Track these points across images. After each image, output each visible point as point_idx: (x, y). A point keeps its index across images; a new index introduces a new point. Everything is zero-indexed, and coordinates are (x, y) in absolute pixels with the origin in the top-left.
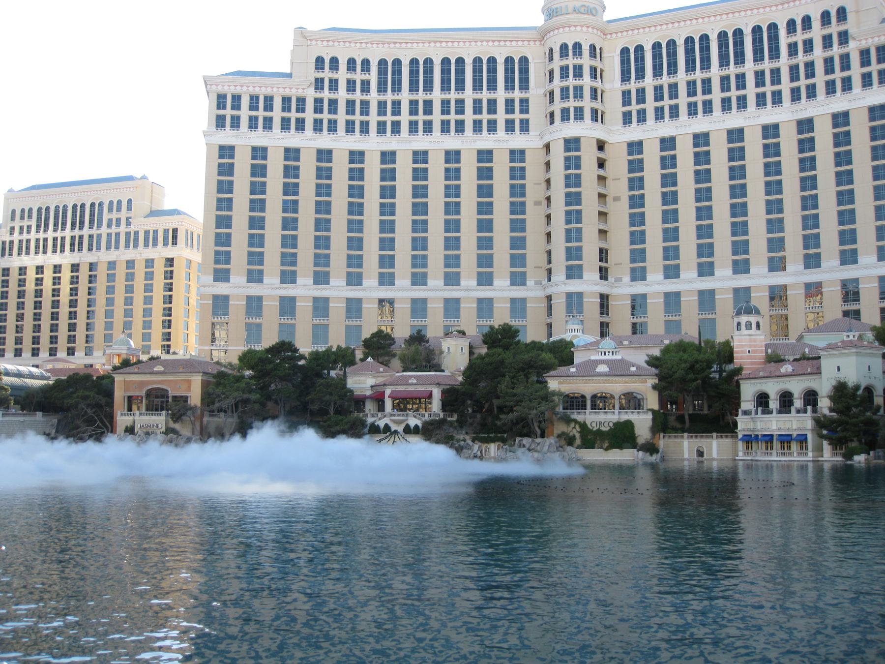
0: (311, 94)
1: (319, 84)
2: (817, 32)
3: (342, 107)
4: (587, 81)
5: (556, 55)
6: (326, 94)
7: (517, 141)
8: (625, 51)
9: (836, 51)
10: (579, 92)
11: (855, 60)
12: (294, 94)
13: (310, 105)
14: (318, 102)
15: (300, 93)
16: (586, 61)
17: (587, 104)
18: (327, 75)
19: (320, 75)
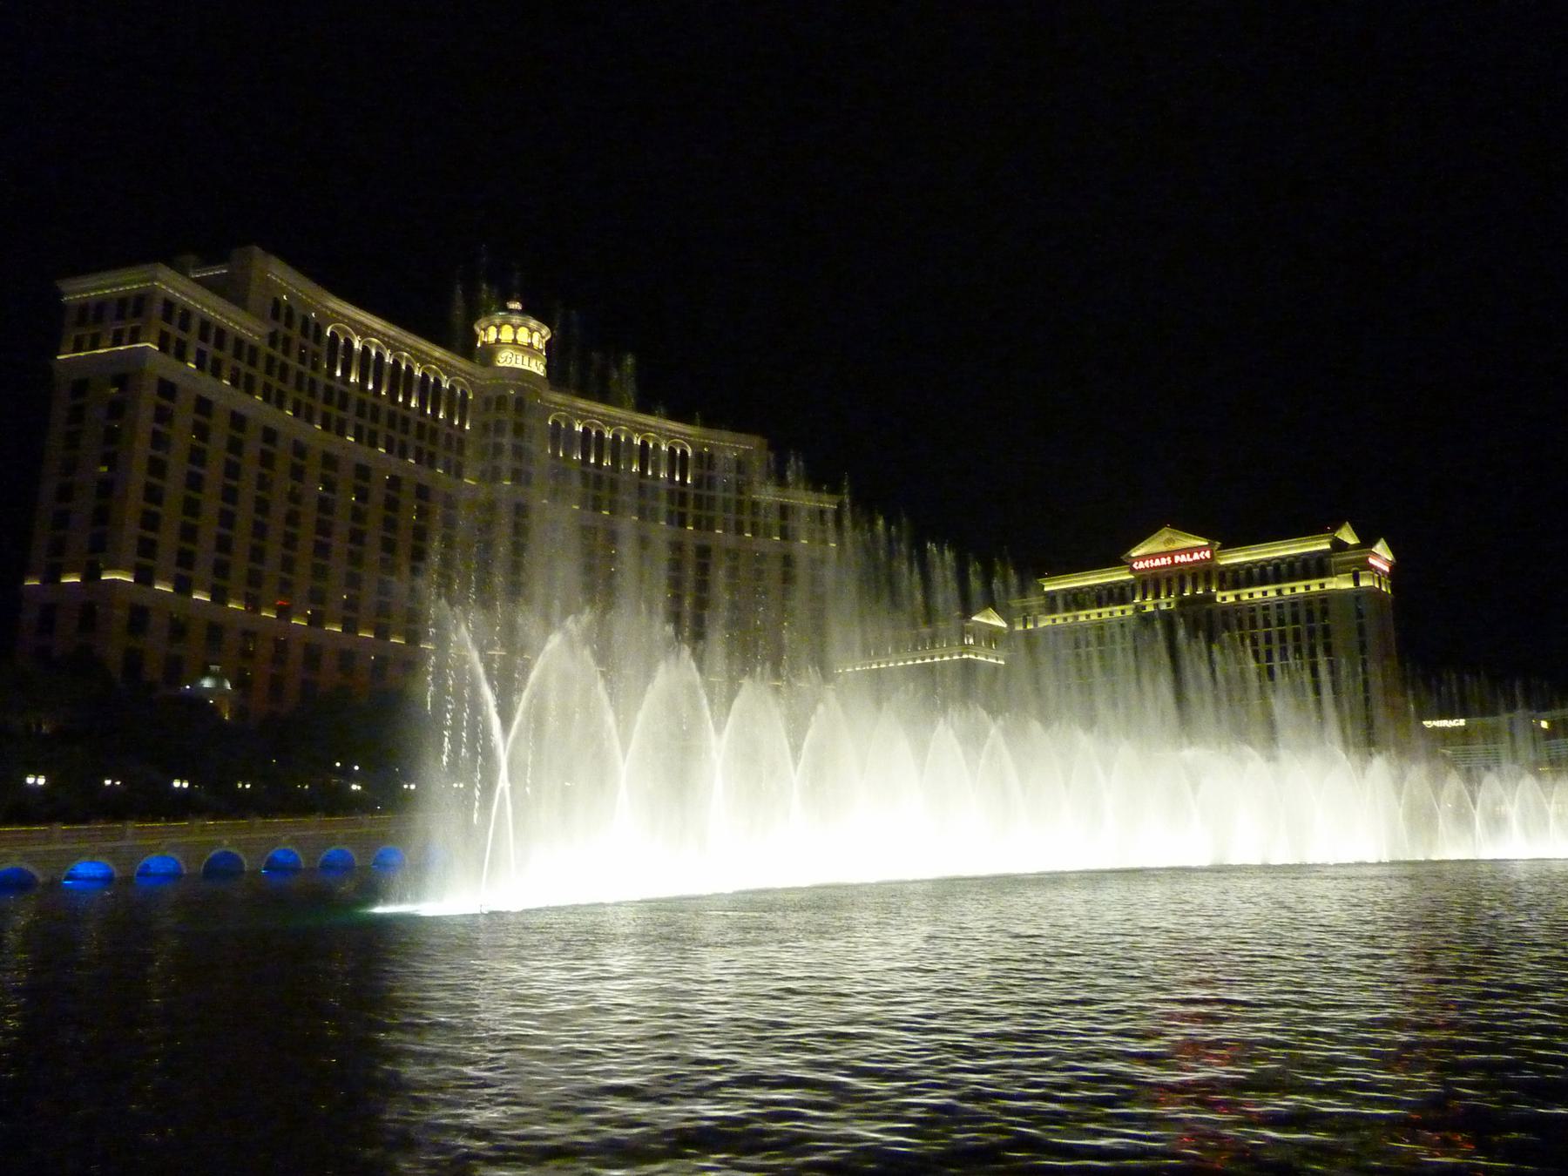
0: (265, 349)
1: (273, 339)
6: (278, 354)
14: (270, 360)
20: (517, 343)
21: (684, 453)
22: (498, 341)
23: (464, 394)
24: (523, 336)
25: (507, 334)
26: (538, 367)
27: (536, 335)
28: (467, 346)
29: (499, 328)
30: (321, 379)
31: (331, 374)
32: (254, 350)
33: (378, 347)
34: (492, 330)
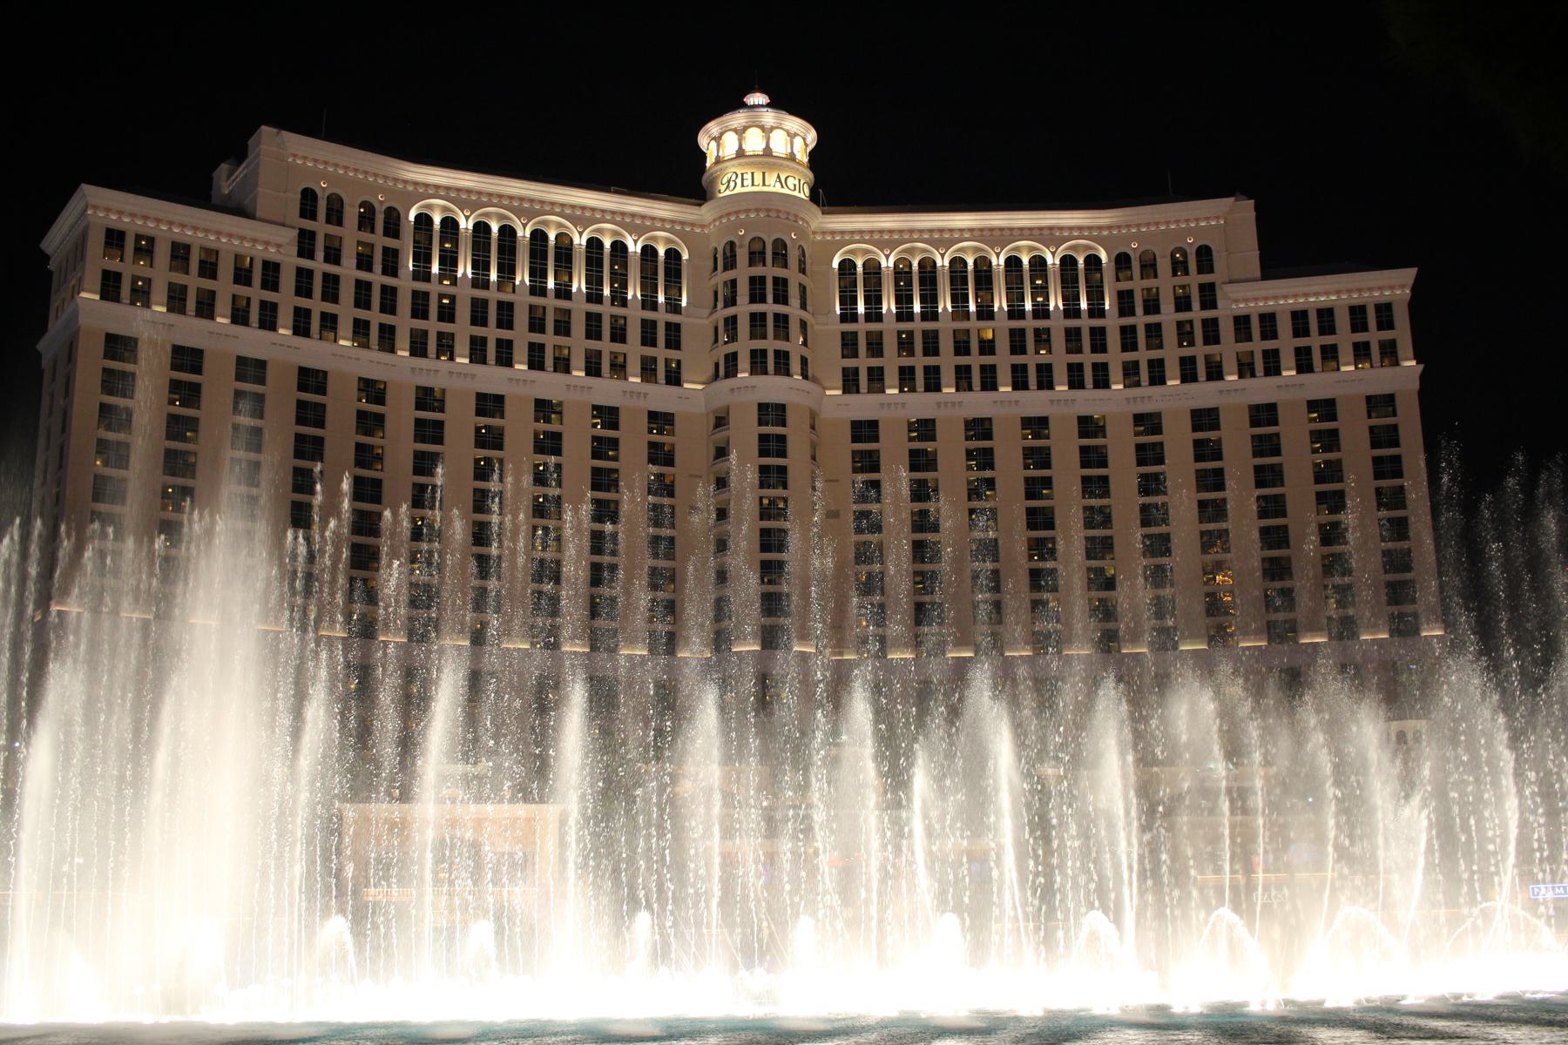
0: (290, 260)
1: (306, 244)
2: (1166, 284)
3: (347, 292)
4: (793, 309)
5: (742, 256)
6: (319, 265)
7: (660, 397)
8: (847, 267)
9: (1197, 314)
10: (782, 321)
11: (1227, 330)
12: (261, 252)
13: (288, 280)
14: (304, 276)
15: (272, 254)
16: (792, 274)
17: (795, 346)
18: (320, 227)
19: (308, 225)
20: (759, 149)
21: (1093, 261)
22: (718, 161)
23: (673, 255)
24: (754, 142)
25: (730, 144)
26: (797, 185)
27: (793, 137)
28: (686, 178)
29: (718, 139)
30: (405, 283)
31: (422, 274)
32: (271, 272)
33: (501, 217)
34: (713, 144)
